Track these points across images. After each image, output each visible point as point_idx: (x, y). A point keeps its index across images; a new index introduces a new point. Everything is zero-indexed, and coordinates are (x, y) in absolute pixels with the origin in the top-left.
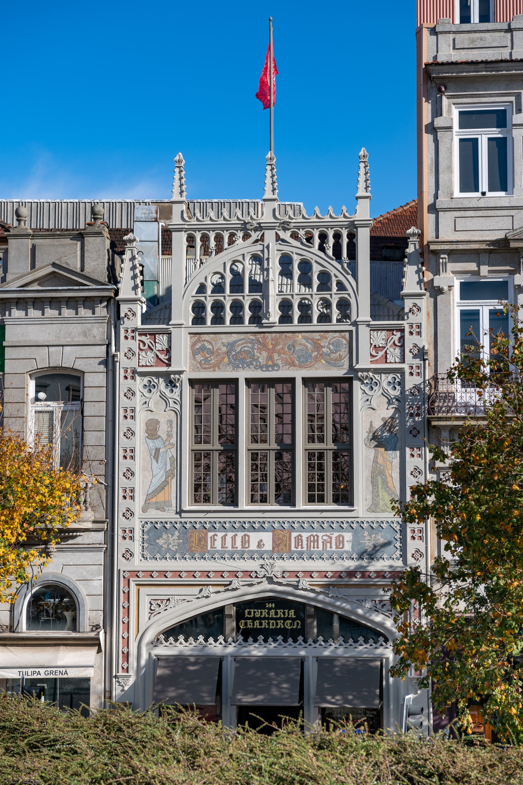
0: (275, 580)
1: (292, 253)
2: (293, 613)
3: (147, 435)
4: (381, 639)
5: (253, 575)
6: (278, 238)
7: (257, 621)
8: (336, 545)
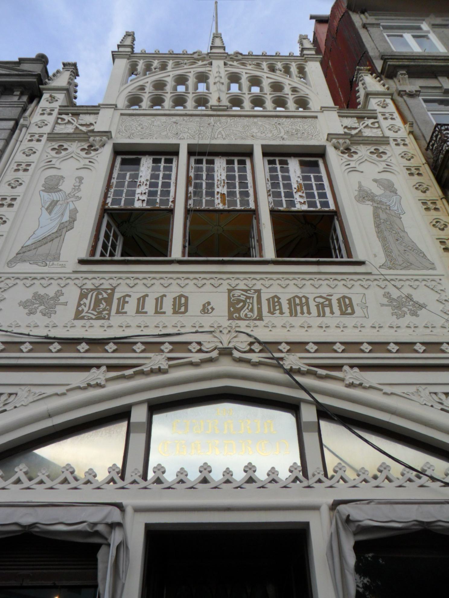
0: (236, 354)
1: (242, 72)
3: (44, 189)
5: (194, 347)
6: (225, 64)
8: (341, 309)
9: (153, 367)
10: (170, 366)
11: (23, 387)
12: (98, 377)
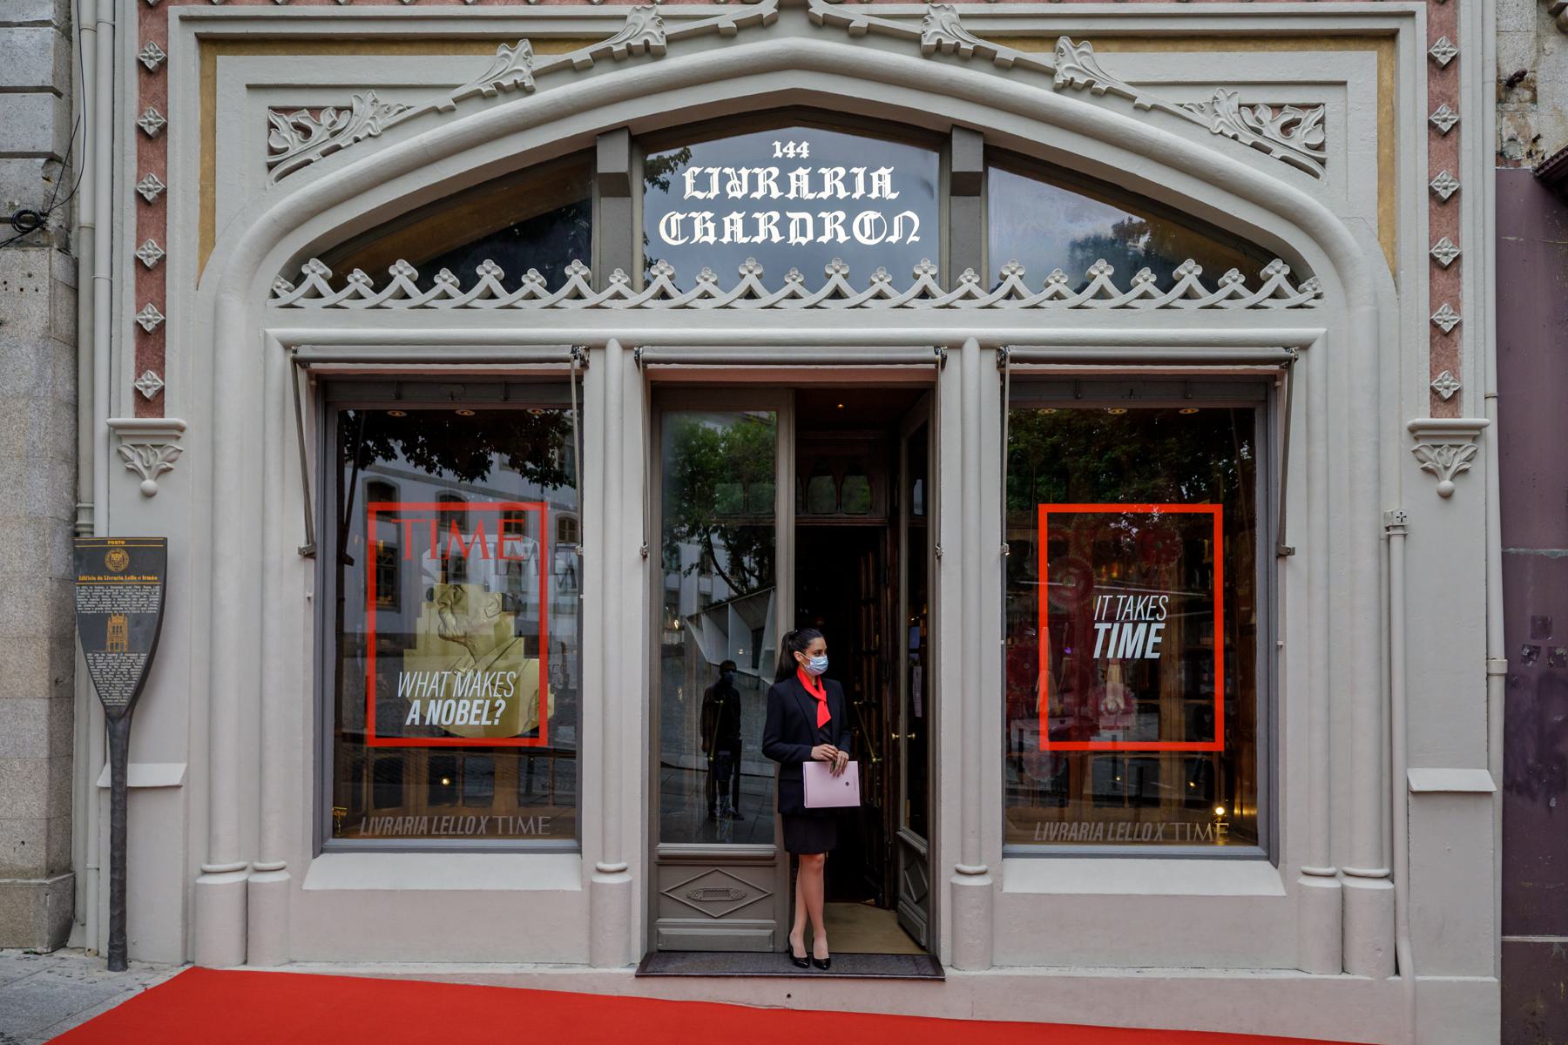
2: (888, 180)
4: (1276, 273)
7: (736, 216)
9: (633, 43)
10: (671, 40)
11: (361, 94)
12: (516, 68)
